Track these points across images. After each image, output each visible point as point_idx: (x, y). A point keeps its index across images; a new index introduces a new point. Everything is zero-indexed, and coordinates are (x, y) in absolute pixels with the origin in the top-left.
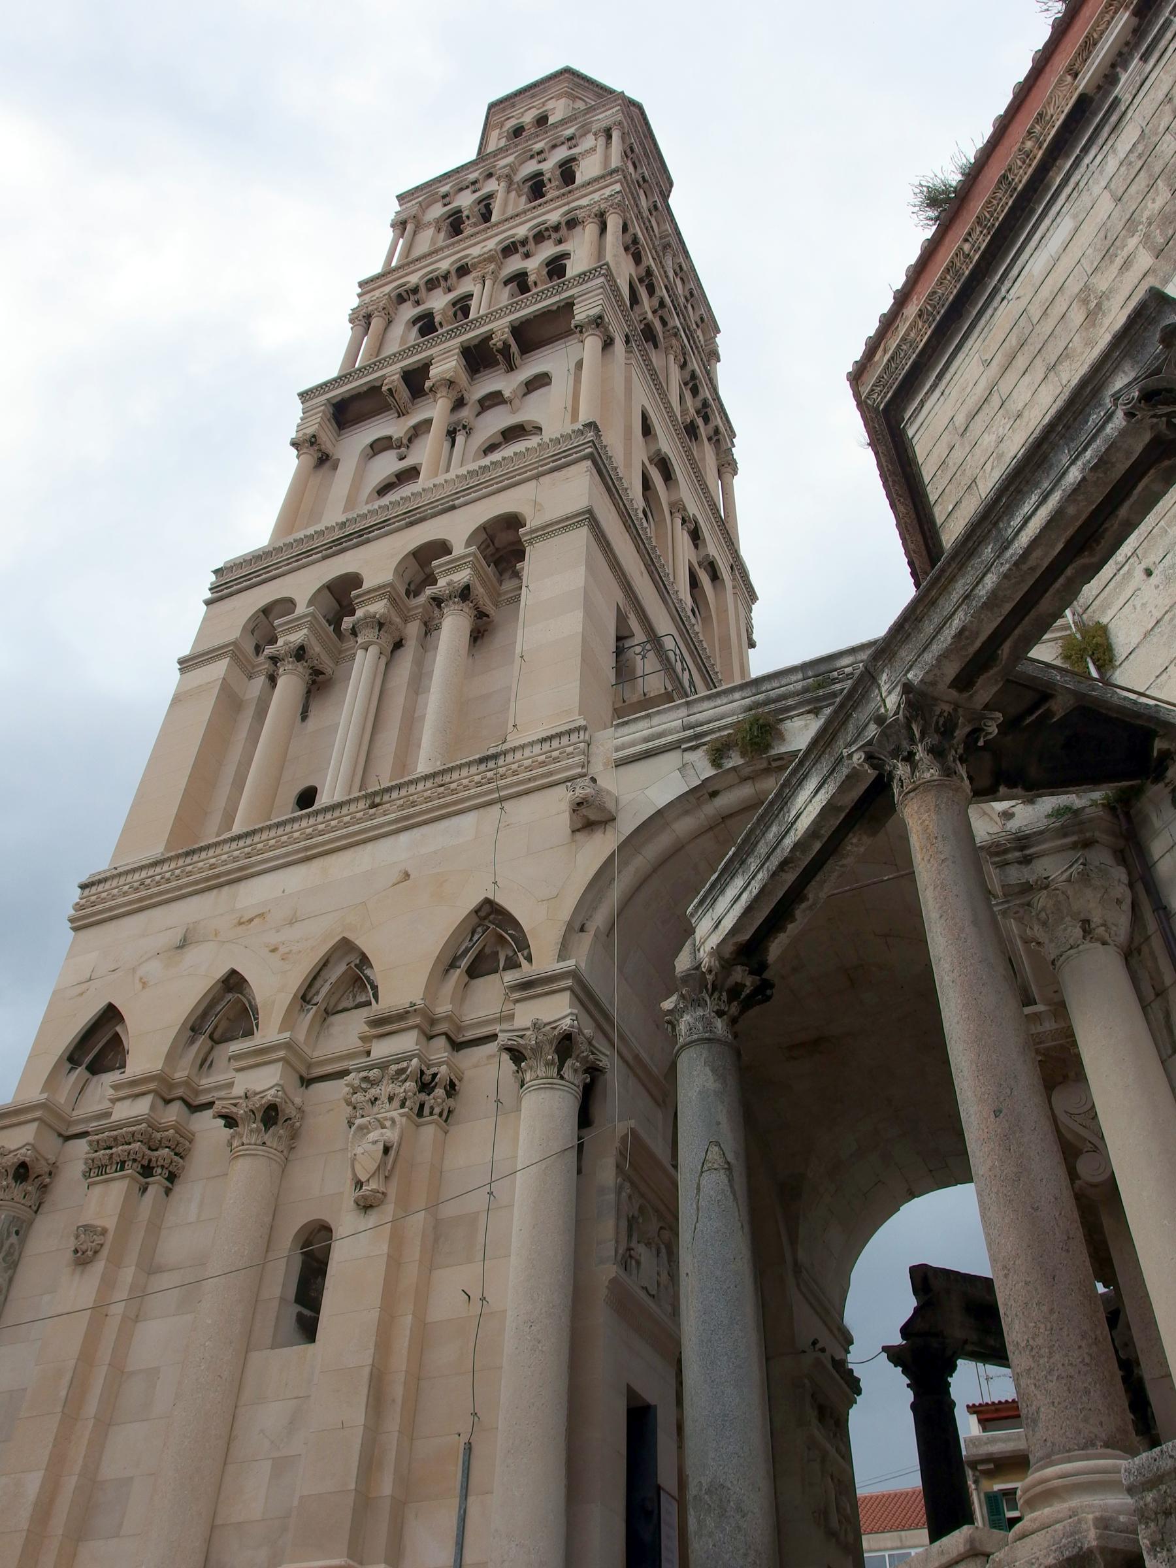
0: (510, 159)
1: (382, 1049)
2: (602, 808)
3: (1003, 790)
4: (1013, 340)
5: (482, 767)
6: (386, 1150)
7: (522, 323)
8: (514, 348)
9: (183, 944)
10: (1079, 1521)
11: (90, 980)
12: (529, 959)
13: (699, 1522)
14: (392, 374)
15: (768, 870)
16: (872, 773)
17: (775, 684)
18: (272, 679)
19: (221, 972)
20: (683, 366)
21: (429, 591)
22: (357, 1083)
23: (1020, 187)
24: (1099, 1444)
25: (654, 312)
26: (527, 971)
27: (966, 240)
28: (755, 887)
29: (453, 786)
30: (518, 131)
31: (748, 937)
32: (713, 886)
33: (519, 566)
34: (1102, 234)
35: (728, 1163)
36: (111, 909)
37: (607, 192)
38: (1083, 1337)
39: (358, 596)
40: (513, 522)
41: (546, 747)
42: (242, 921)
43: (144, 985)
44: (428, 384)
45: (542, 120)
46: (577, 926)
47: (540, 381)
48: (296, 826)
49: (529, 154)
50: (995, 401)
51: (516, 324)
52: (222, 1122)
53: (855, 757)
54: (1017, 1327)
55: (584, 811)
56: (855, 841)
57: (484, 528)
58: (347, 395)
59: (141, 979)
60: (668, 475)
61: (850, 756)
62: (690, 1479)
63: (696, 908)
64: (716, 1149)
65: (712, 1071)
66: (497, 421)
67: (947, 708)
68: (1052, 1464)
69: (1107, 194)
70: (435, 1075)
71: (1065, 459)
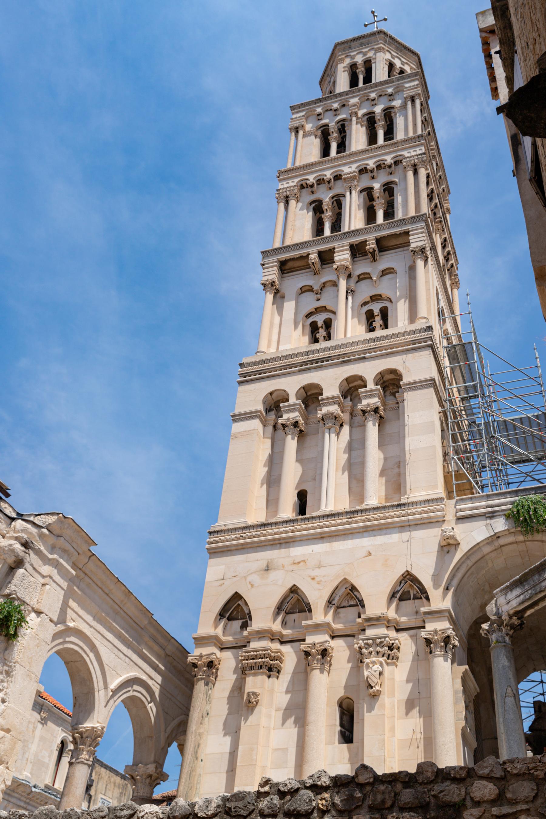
7: (381, 238)
8: (377, 252)
19: (290, 586)
43: (252, 586)
49: (366, 98)
51: (378, 237)
58: (288, 258)
59: (250, 582)
64: (510, 689)
65: (507, 658)
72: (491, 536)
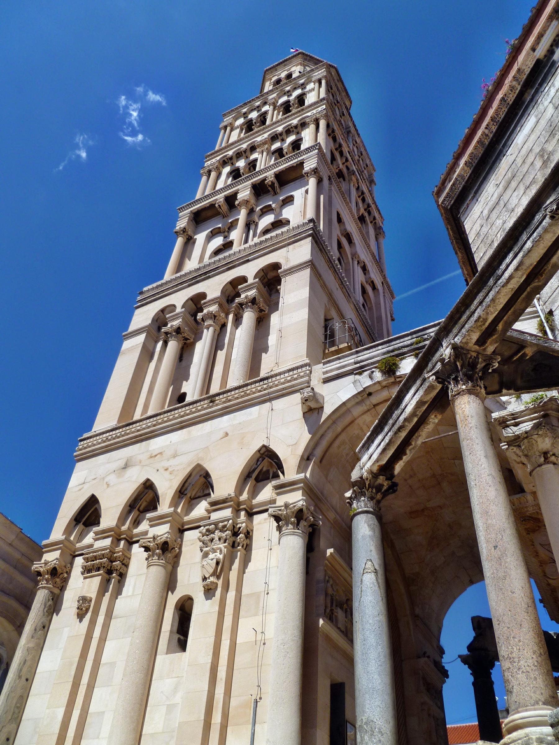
0: (275, 95)
1: (215, 516)
2: (317, 401)
3: (504, 391)
4: (509, 175)
5: (261, 383)
6: (218, 563)
8: (276, 185)
9: (126, 467)
10: (529, 739)
11: (84, 483)
12: (283, 473)
13: (361, 737)
14: (220, 198)
15: (393, 431)
16: (440, 386)
17: (398, 341)
18: (166, 343)
19: (142, 480)
20: (358, 189)
21: (237, 300)
22: (204, 531)
23: (511, 103)
24: (541, 703)
25: (343, 164)
26: (283, 479)
27: (486, 128)
28: (387, 440)
29: (248, 392)
30: (278, 81)
31: (384, 463)
32: (369, 438)
33: (279, 287)
34: (549, 124)
35: (375, 569)
36: (93, 451)
37: (320, 109)
38: (534, 653)
39: (205, 303)
40: (276, 266)
41: (291, 373)
42: (152, 455)
43: (108, 485)
44: (237, 202)
45: (289, 76)
46: (306, 457)
47: (289, 200)
48: (176, 412)
49: (283, 93)
50: (502, 203)
51: (277, 173)
52: (143, 549)
53: (431, 378)
54: (503, 649)
55: (308, 403)
56: (433, 417)
57: (263, 270)
58: (200, 208)
59: (107, 483)
60: (350, 241)
61: (429, 377)
62: (358, 717)
63: (360, 450)
64: (370, 563)
65: (368, 526)
66: (269, 219)
67: (474, 354)
68: (518, 712)
69: (551, 105)
70: (240, 528)
71: (524, 237)
72: (359, 393)
